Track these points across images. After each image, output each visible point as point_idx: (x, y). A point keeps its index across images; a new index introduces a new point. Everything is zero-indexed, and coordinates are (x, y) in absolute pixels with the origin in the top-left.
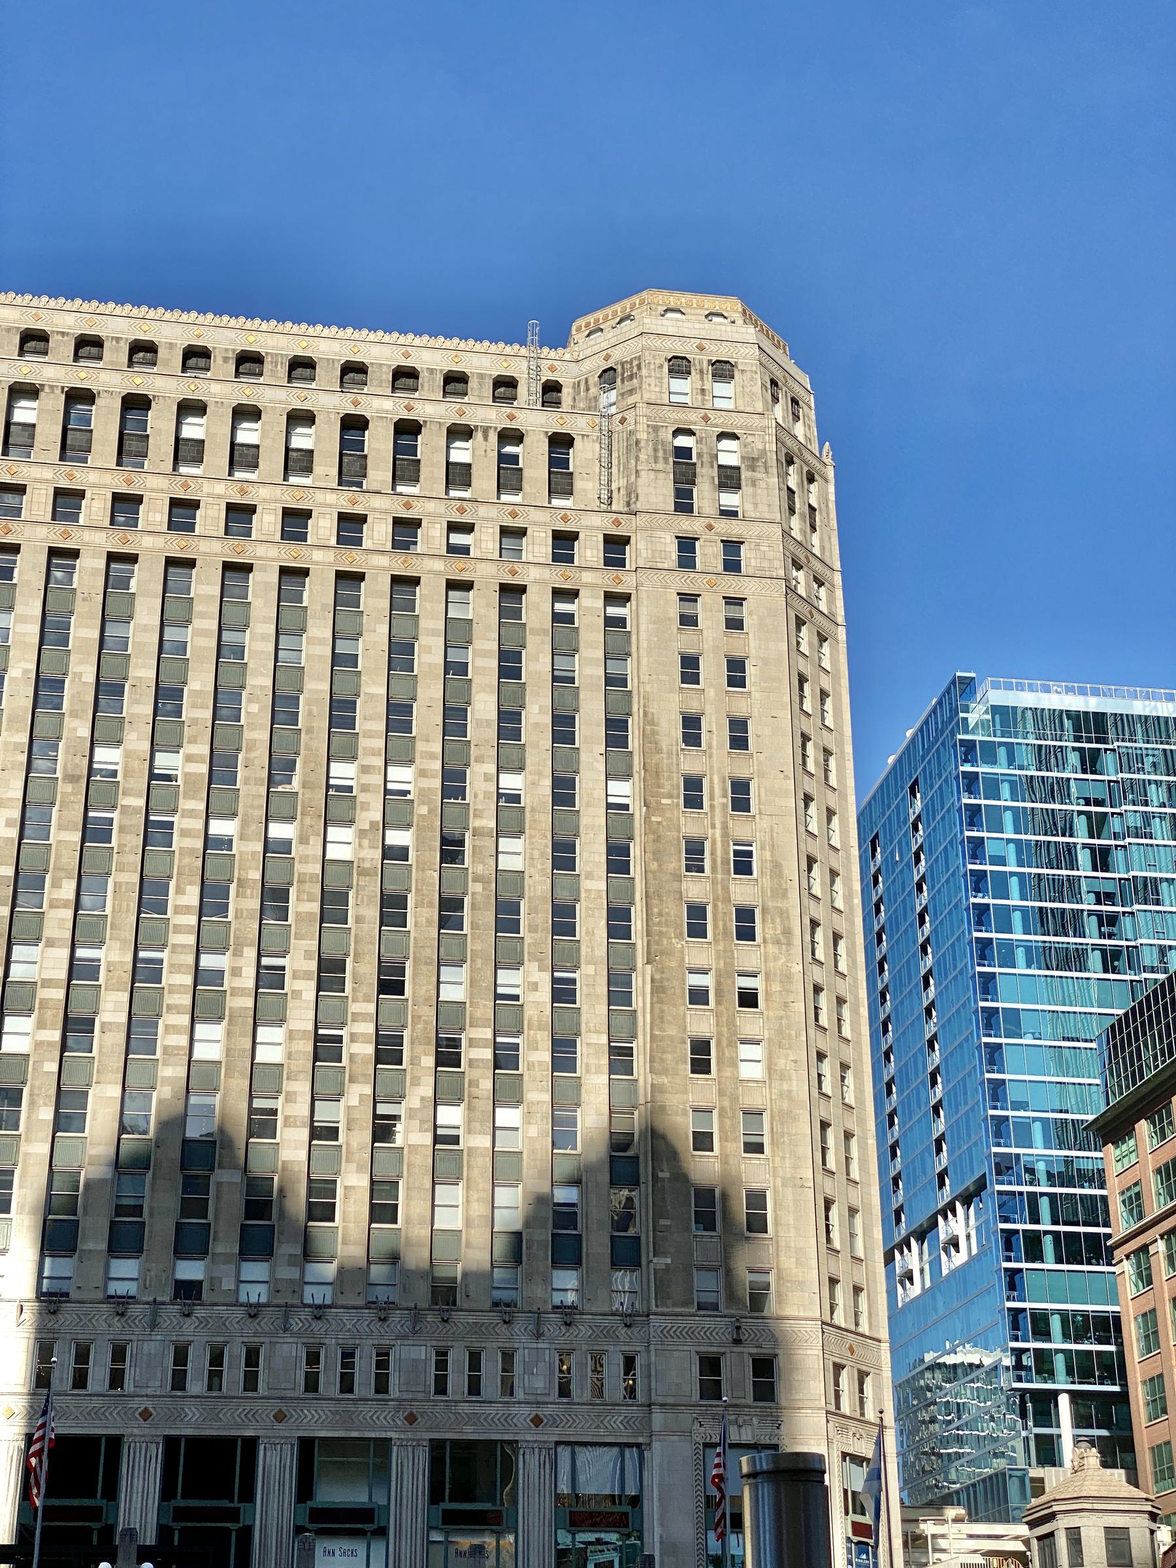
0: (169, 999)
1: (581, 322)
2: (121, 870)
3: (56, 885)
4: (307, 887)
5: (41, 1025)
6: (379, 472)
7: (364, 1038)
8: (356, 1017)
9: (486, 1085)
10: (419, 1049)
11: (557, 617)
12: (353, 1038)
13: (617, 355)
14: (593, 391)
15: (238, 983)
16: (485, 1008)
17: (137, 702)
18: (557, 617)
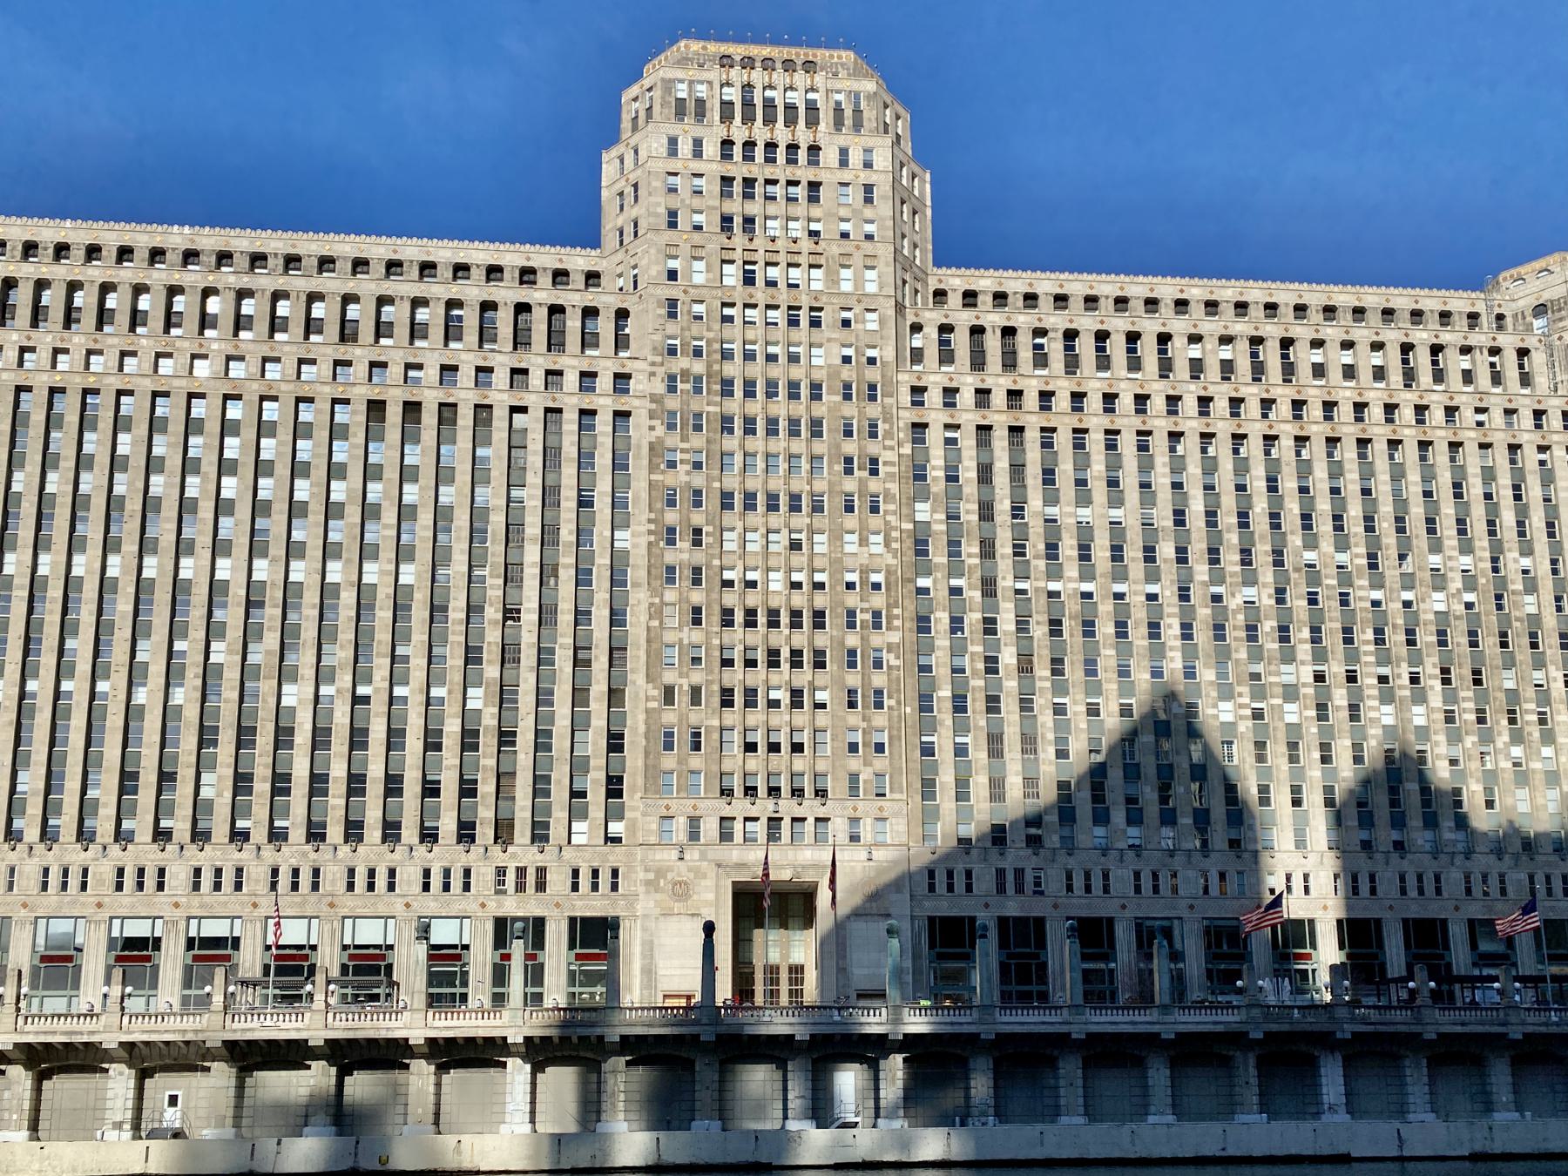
0: (1367, 692)
1: (1506, 274)
2: (1330, 620)
3: (1300, 630)
4: (1429, 627)
5: (1306, 708)
6: (1425, 377)
7: (1470, 711)
8: (1464, 699)
9: (1537, 735)
10: (1499, 715)
11: (1542, 463)
12: (1465, 711)
13: (1546, 297)
14: (1529, 319)
15: (1398, 682)
16: (1530, 692)
17: (1324, 524)
18: (1542, 463)
